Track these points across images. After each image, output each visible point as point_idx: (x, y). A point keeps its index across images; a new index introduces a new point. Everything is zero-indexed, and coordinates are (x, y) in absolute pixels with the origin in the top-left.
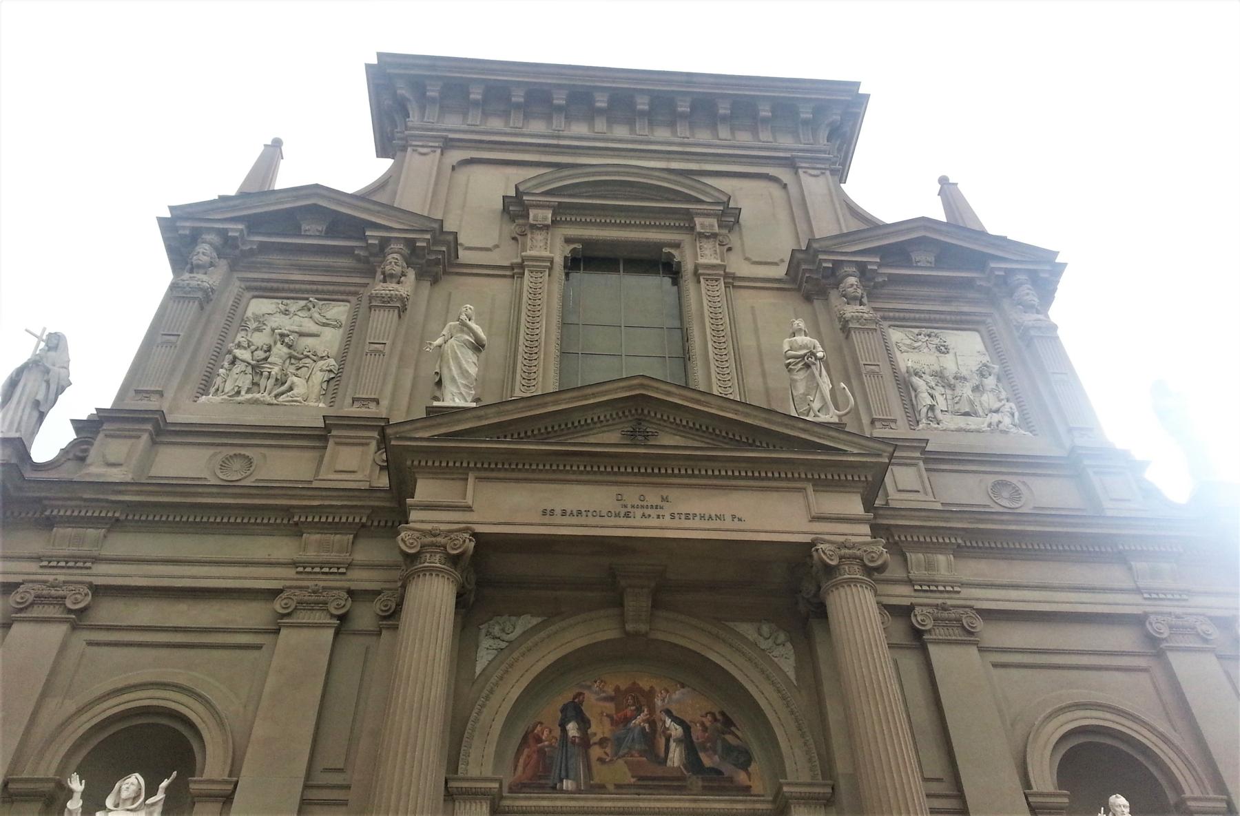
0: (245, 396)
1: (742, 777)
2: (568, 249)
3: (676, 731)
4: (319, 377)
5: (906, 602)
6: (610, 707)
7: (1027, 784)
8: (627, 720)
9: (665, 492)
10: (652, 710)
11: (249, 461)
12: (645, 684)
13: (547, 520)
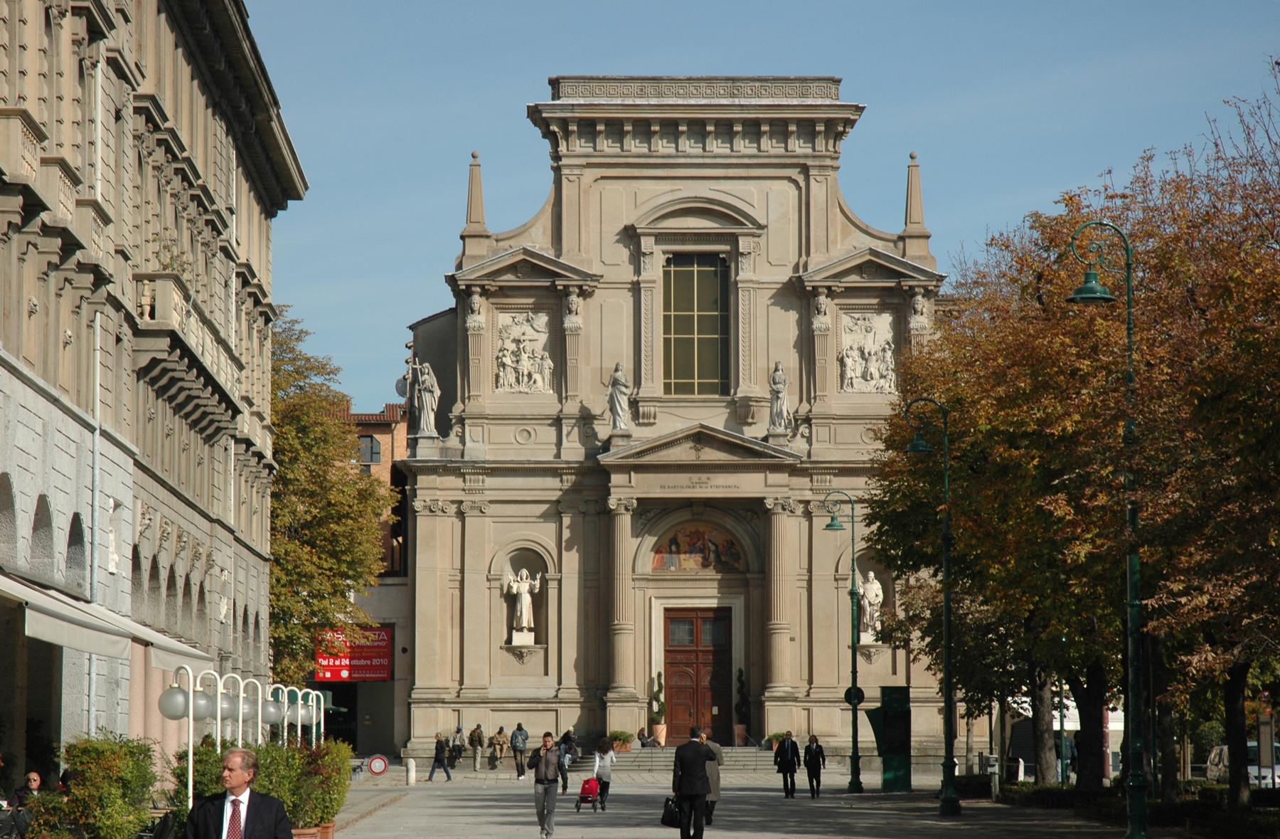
0: (517, 388)
1: (736, 565)
2: (667, 256)
3: (713, 548)
4: (547, 372)
5: (807, 498)
6: (688, 539)
7: (837, 571)
8: (694, 544)
9: (709, 475)
10: (704, 539)
11: (529, 433)
12: (701, 529)
13: (663, 490)
